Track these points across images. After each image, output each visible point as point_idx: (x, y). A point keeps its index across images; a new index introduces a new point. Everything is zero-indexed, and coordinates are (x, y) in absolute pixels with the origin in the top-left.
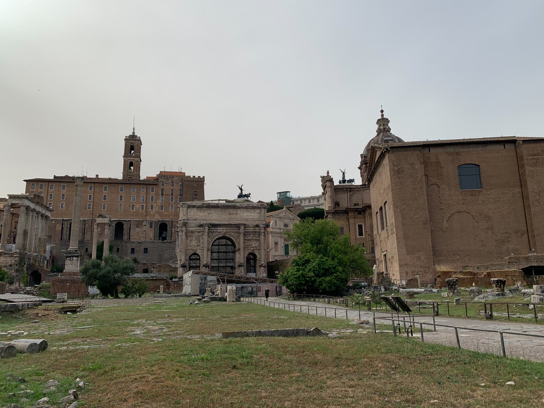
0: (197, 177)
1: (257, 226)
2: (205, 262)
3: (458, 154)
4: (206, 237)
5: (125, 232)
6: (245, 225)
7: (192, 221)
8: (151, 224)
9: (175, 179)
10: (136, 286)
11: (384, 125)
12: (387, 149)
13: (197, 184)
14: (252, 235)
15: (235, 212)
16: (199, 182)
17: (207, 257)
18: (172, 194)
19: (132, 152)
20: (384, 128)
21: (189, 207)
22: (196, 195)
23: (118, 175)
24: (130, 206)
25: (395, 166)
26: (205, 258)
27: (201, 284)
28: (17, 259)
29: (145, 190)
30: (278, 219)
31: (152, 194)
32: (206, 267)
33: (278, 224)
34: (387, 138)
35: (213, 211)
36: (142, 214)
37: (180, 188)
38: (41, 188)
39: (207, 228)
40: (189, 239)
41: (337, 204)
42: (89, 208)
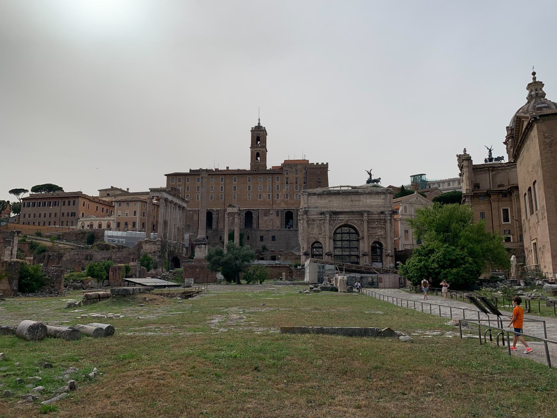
0: (320, 164)
1: (382, 213)
2: (328, 251)
4: (327, 226)
5: (254, 221)
6: (368, 212)
7: (313, 209)
8: (278, 212)
9: (299, 167)
10: (258, 273)
11: (536, 90)
12: (535, 118)
13: (321, 171)
14: (376, 223)
15: (357, 199)
16: (323, 169)
17: (330, 245)
18: (296, 183)
19: (259, 142)
20: (537, 94)
21: (309, 194)
22: (319, 182)
23: (246, 166)
24: (257, 196)
25: (546, 138)
26: (328, 246)
27: (319, 272)
28: (159, 246)
29: (270, 179)
30: (407, 205)
31: (278, 183)
32: (329, 255)
33: (408, 209)
34: (539, 106)
35: (334, 198)
39: (328, 216)
41: (477, 186)
42: (222, 199)
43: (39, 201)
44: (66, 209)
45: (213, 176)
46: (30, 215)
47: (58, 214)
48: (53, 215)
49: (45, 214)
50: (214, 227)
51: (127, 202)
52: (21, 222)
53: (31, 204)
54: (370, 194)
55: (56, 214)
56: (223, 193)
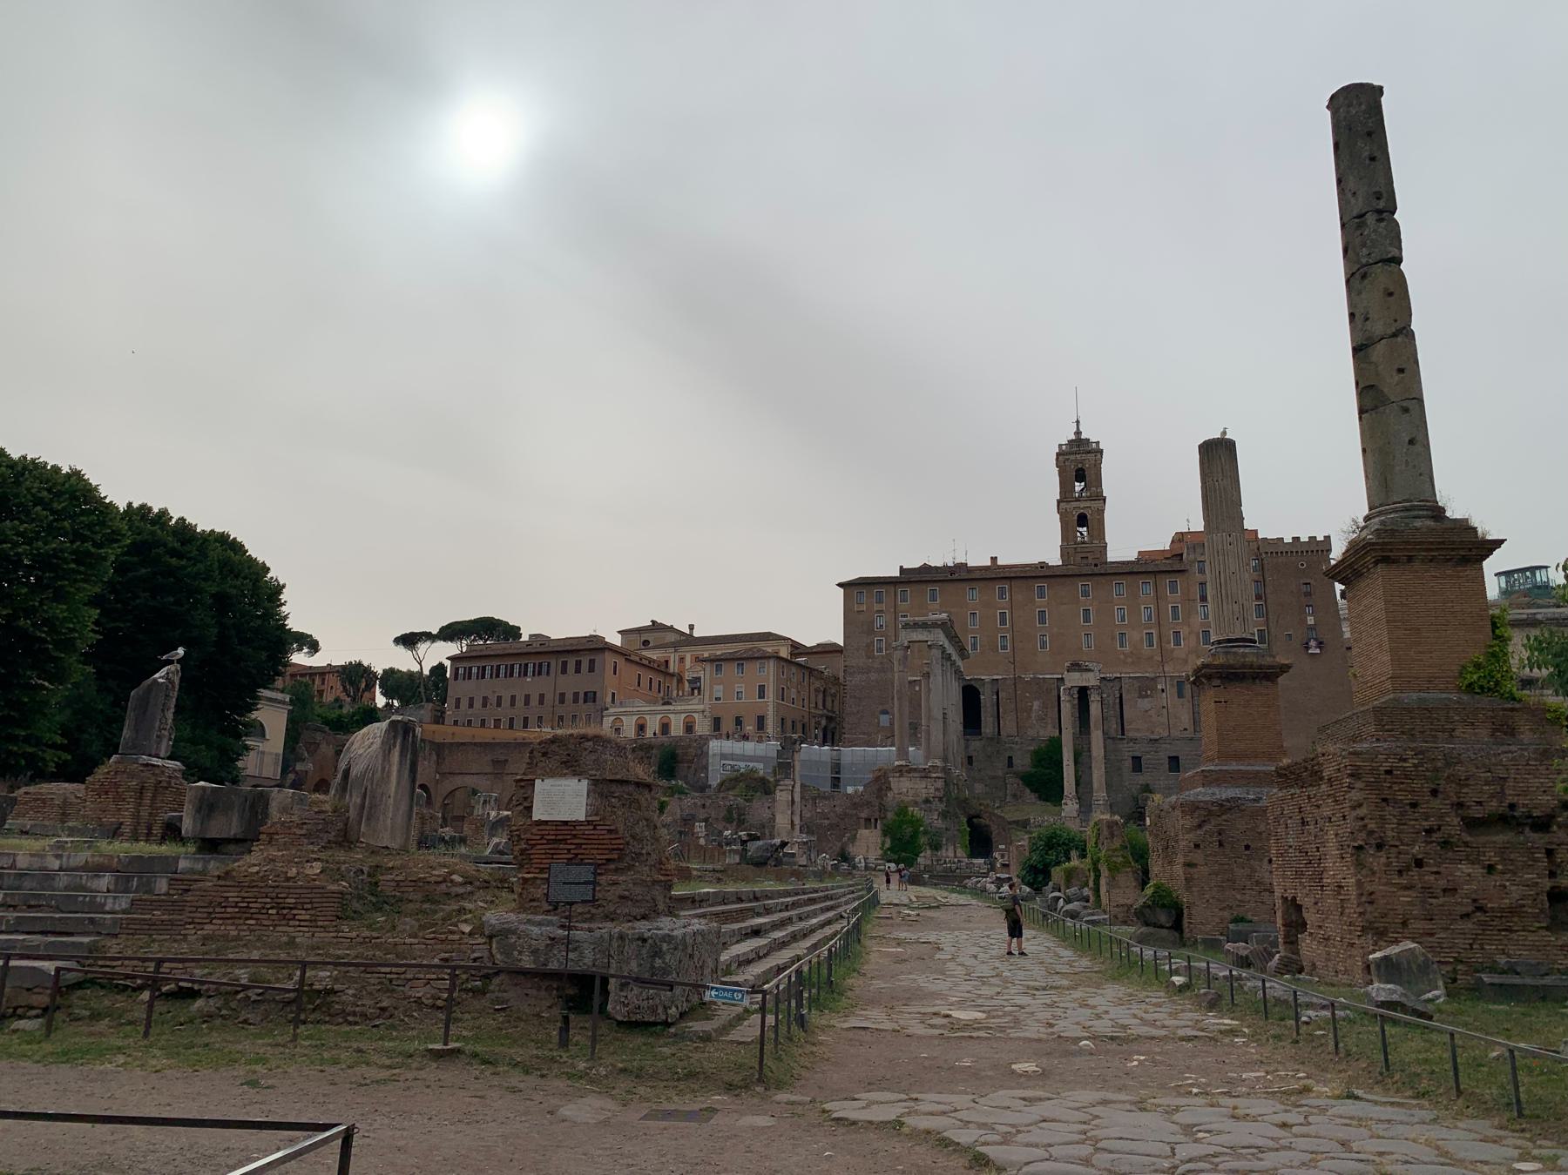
0: (1304, 539)
8: (1180, 685)
22: (1308, 594)
24: (1113, 638)
28: (940, 784)
29: (1150, 590)
37: (1255, 575)
38: (880, 601)
42: (1004, 647)
43: (495, 664)
44: (572, 683)
45: (974, 585)
46: (471, 700)
47: (548, 698)
48: (534, 701)
49: (513, 697)
50: (988, 727)
51: (739, 660)
52: (449, 720)
53: (475, 670)
55: (542, 696)
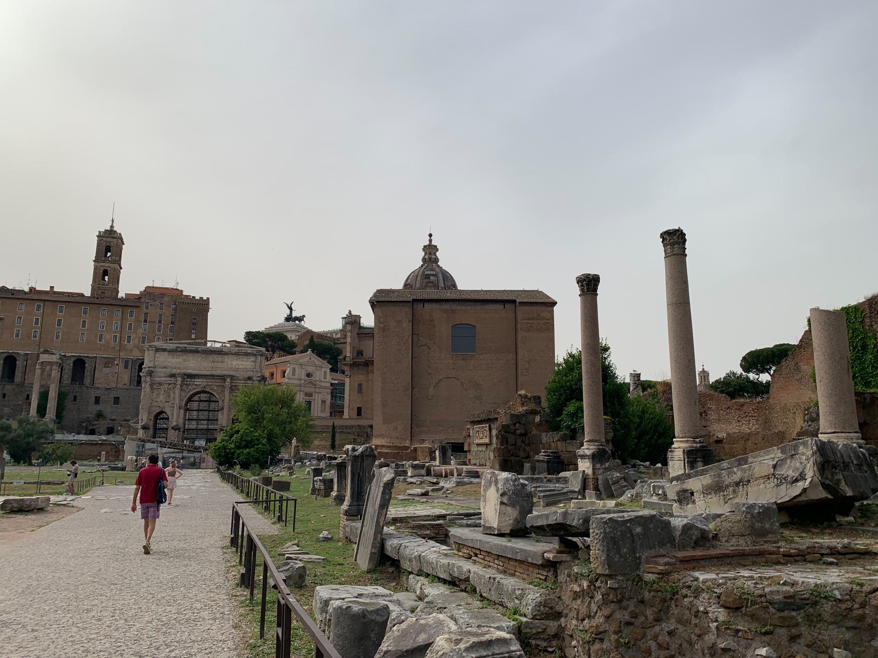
1: (250, 378)
2: (175, 424)
3: (454, 311)
4: (177, 391)
5: (87, 373)
9: (166, 299)
10: (59, 452)
13: (198, 310)
16: (201, 307)
18: (160, 322)
19: (109, 254)
20: (430, 259)
21: (158, 350)
22: (194, 324)
24: (96, 336)
26: (176, 417)
29: (120, 314)
30: (297, 367)
31: (131, 319)
32: (175, 430)
34: (429, 272)
36: (114, 348)
37: (172, 312)
39: (179, 379)
40: (156, 391)
42: (35, 337)
45: (22, 301)
50: (18, 378)
54: (236, 354)
56: (38, 328)
